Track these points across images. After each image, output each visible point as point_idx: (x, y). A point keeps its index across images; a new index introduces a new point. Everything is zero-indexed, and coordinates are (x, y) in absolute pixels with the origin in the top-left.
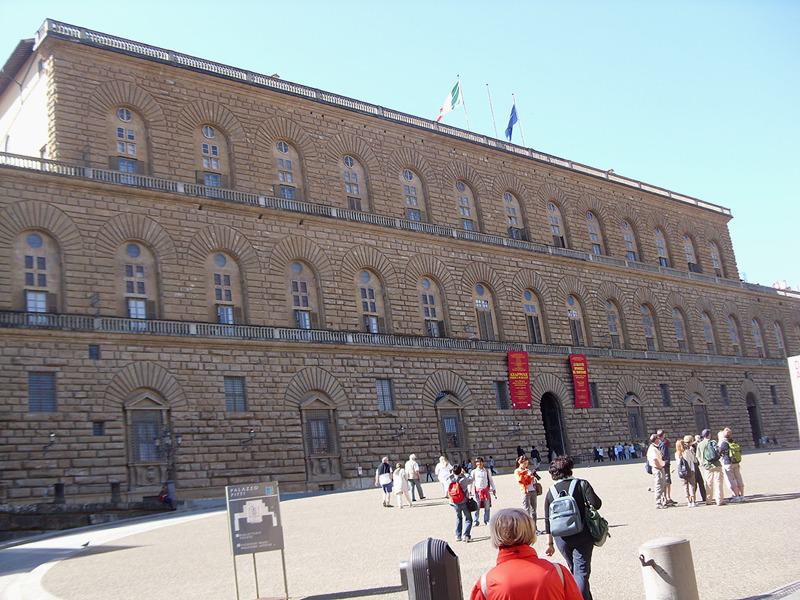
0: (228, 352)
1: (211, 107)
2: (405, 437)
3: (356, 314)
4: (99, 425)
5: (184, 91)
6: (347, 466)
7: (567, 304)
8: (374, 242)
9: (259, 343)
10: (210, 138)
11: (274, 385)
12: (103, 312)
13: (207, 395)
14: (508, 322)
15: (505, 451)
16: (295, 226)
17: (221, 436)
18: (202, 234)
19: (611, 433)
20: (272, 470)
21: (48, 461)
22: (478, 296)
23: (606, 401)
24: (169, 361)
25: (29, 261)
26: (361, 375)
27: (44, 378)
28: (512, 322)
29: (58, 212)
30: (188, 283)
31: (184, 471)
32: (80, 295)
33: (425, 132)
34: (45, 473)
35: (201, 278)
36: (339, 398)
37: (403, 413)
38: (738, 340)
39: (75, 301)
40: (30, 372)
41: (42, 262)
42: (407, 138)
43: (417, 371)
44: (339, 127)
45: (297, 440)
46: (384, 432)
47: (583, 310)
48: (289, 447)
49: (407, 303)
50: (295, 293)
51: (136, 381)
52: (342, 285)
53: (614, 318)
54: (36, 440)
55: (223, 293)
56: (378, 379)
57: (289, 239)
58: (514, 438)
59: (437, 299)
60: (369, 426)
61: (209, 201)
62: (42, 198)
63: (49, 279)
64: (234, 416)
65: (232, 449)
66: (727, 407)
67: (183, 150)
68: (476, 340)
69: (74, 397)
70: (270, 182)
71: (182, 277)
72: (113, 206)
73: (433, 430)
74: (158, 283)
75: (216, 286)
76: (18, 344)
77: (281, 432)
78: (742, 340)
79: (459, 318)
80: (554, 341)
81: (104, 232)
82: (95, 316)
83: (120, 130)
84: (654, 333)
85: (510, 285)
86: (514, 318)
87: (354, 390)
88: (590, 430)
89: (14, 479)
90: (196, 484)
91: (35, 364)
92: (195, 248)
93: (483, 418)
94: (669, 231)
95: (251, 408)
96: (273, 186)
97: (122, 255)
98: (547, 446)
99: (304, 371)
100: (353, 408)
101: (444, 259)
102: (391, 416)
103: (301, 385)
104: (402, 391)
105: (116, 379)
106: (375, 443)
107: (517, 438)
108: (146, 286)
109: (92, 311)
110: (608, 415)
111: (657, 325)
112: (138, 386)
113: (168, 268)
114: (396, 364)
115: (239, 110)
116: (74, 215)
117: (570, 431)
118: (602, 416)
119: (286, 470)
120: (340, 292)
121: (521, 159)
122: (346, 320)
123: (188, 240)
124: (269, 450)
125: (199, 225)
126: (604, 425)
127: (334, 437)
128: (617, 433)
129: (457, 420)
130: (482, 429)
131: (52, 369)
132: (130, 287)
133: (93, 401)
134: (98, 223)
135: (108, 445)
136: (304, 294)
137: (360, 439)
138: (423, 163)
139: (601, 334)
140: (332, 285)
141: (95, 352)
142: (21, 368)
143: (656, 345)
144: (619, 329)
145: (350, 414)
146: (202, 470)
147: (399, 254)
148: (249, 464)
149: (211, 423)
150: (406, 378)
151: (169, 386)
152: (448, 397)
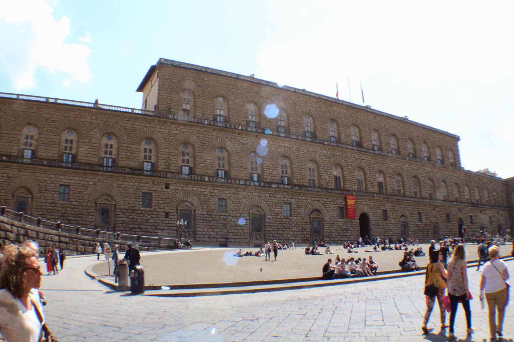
0: (221, 189)
3: (278, 175)
4: (167, 215)
5: (211, 83)
6: (268, 238)
8: (288, 146)
12: (171, 170)
15: (340, 237)
16: (254, 138)
17: (215, 222)
18: (214, 140)
19: (391, 232)
20: (235, 237)
24: (196, 191)
25: (146, 150)
29: (157, 132)
30: (206, 160)
31: (199, 234)
32: (163, 164)
34: (146, 230)
36: (267, 209)
37: (295, 218)
39: (161, 166)
40: (143, 193)
41: (150, 151)
42: (308, 101)
43: (303, 201)
47: (385, 178)
53: (400, 182)
54: (144, 218)
55: (221, 165)
56: (285, 203)
57: (251, 143)
58: (345, 232)
63: (153, 158)
64: (221, 214)
66: (448, 224)
68: (332, 189)
69: (158, 203)
70: (244, 119)
73: (308, 226)
74: (195, 160)
75: (218, 162)
80: (368, 191)
82: (168, 172)
83: (185, 99)
84: (418, 190)
87: (274, 207)
91: (145, 190)
92: (210, 147)
94: (430, 144)
96: (246, 121)
97: (181, 148)
99: (252, 198)
100: (273, 214)
102: (289, 219)
104: (295, 208)
105: (175, 197)
106: (281, 229)
107: (346, 231)
109: (167, 170)
111: (420, 186)
115: (234, 90)
117: (372, 230)
118: (388, 224)
122: (273, 178)
123: (208, 143)
124: (234, 229)
128: (394, 232)
129: (319, 223)
131: (151, 192)
132: (183, 161)
135: (170, 222)
140: (268, 163)
141: (167, 187)
142: (140, 191)
144: (401, 187)
145: (271, 217)
146: (206, 234)
149: (211, 216)
152: (316, 212)
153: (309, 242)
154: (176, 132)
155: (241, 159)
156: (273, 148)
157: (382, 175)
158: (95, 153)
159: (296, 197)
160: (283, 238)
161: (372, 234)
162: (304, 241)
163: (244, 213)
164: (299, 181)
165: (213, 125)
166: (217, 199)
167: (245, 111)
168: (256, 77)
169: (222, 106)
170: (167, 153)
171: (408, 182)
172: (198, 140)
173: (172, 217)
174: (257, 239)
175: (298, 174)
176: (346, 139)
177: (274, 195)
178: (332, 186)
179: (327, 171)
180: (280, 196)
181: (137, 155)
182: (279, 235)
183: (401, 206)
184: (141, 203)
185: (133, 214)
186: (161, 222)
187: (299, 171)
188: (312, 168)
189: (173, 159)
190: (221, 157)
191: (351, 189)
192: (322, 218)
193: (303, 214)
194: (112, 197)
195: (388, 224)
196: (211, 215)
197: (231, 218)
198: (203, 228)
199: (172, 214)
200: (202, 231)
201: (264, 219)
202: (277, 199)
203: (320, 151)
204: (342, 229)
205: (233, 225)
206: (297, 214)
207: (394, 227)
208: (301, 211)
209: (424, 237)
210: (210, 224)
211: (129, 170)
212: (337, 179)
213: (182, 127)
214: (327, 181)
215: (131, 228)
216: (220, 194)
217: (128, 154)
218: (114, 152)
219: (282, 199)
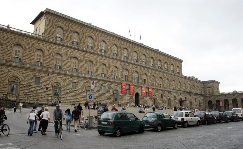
12: (50, 67)
13: (69, 85)
20: (79, 101)
25: (38, 55)
27: (38, 78)
32: (47, 63)
37: (107, 93)
39: (45, 64)
40: (35, 77)
54: (35, 90)
59: (117, 72)
78: (181, 87)
89: (30, 97)
94: (168, 63)
109: (48, 66)
113: (64, 60)
114: (106, 83)
119: (82, 101)
122: (98, 74)
125: (72, 52)
135: (49, 92)
141: (48, 75)
143: (162, 86)
145: (96, 92)
152: (116, 91)
154: (54, 48)
157: (146, 76)
164: (109, 76)
168: (92, 24)
177: (98, 82)
179: (122, 72)
194: (18, 78)
197: (78, 91)
213: (57, 46)
218: (21, 55)
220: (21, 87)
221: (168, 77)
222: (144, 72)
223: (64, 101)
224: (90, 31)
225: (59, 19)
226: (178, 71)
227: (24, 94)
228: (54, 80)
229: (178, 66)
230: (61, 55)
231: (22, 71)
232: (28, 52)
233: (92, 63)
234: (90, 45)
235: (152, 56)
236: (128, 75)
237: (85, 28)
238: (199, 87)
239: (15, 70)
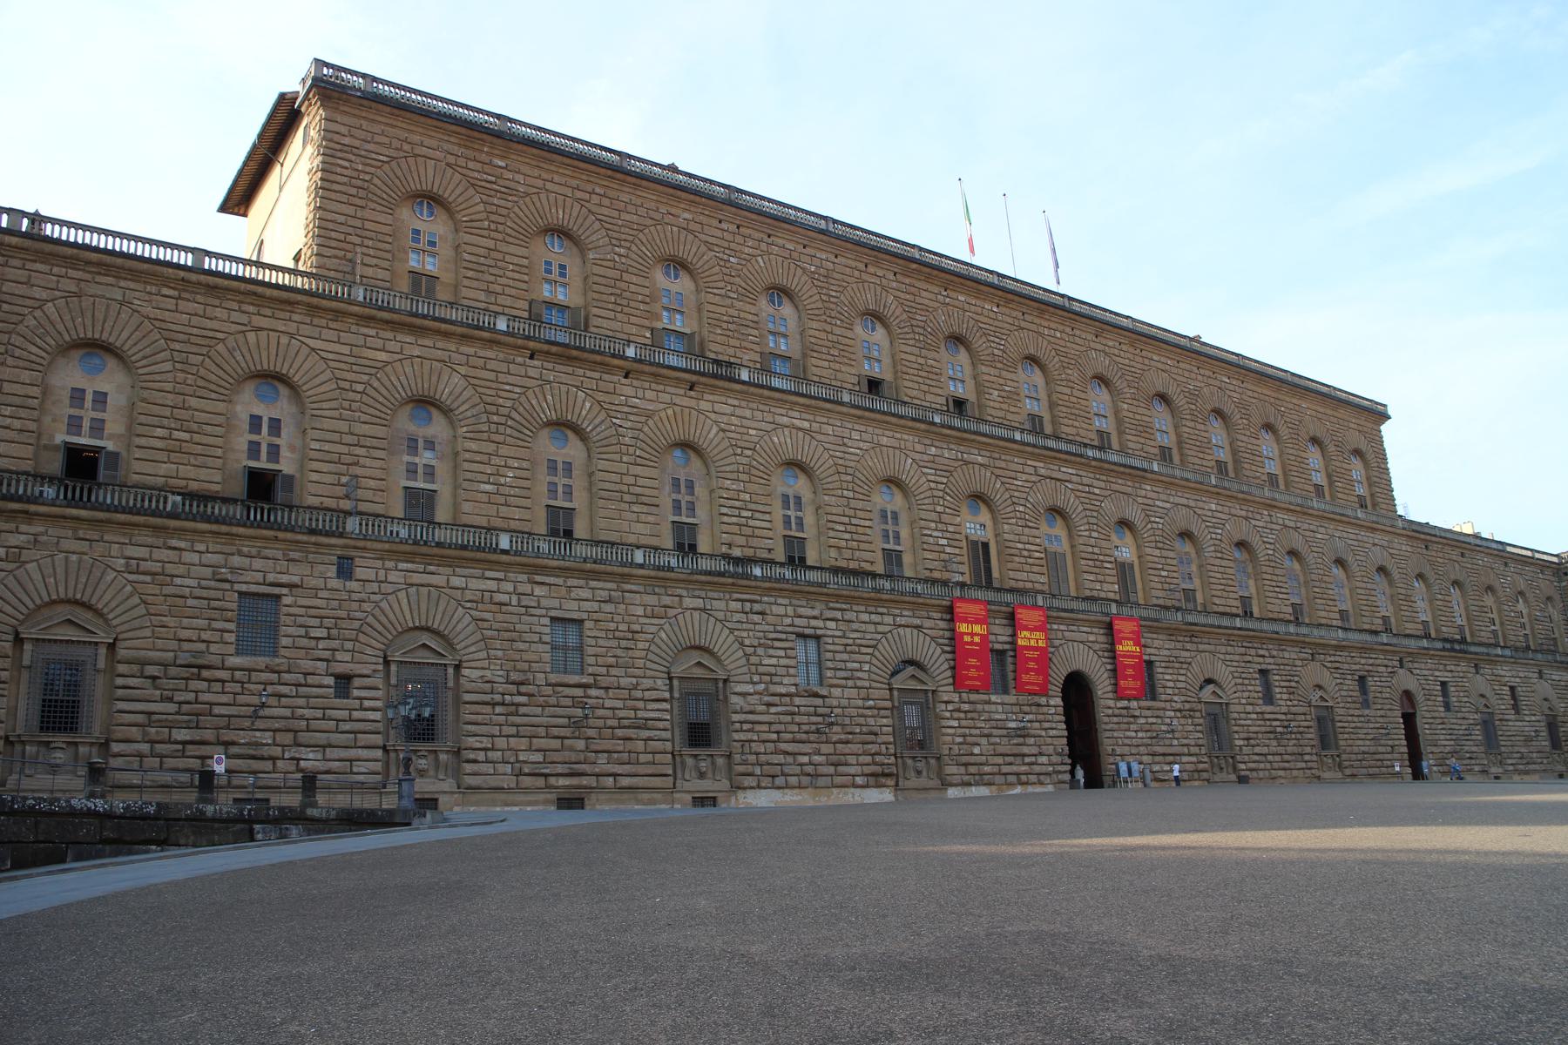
0: (560, 581)
1: (560, 203)
2: (835, 729)
6: (741, 769)
7: (1114, 537)
8: (806, 425)
9: (609, 568)
10: (554, 251)
11: (630, 636)
12: (363, 507)
13: (521, 646)
14: (1017, 559)
15: (1000, 760)
16: (682, 392)
21: (258, 734)
22: (969, 517)
23: (1169, 691)
26: (772, 628)
28: (1023, 560)
29: (305, 350)
30: (503, 471)
31: (475, 761)
33: (901, 262)
34: (251, 752)
35: (525, 464)
36: (733, 660)
37: (837, 692)
38: (1391, 608)
40: (241, 593)
41: (275, 426)
44: (763, 246)
45: (661, 725)
46: (805, 719)
48: (645, 734)
49: (854, 521)
50: (674, 496)
51: (408, 617)
52: (751, 487)
54: (241, 699)
55: (560, 489)
56: (800, 635)
57: (670, 412)
58: (1015, 741)
60: (779, 709)
61: (546, 347)
62: (283, 329)
63: (285, 452)
65: (555, 731)
66: (1367, 712)
67: (511, 267)
69: (307, 636)
70: (647, 323)
71: (495, 460)
72: (392, 346)
76: (227, 549)
77: (636, 709)
78: (1398, 609)
79: (937, 548)
80: (1088, 593)
81: (376, 384)
83: (417, 232)
84: (1253, 590)
85: (1022, 502)
86: (1026, 553)
87: (760, 651)
88: (1140, 735)
90: (494, 784)
92: (518, 417)
93: (966, 707)
94: (1284, 431)
95: (590, 670)
96: (652, 330)
98: (1069, 756)
99: (680, 617)
100: (756, 678)
101: (918, 456)
102: (816, 695)
103: (674, 639)
104: (838, 657)
105: (377, 612)
107: (1021, 740)
108: (438, 472)
109: (346, 505)
110: (1172, 714)
112: (411, 625)
113: (473, 446)
115: (605, 211)
116: (331, 356)
118: (1161, 713)
120: (747, 497)
121: (1052, 310)
122: (755, 542)
123: (509, 403)
126: (1164, 728)
127: (723, 723)
128: (1185, 741)
130: (964, 723)
131: (276, 590)
133: (335, 644)
134: (367, 370)
135: (356, 714)
136: (689, 498)
137: (765, 728)
138: (893, 307)
139: (1166, 587)
140: (734, 487)
141: (345, 569)
142: (227, 586)
145: (750, 688)
147: (844, 445)
148: (582, 757)
149: (523, 689)
150: (843, 637)
151: (460, 626)
152: (910, 670)
153: (891, 782)
154: (383, 356)
155: (638, 470)
156: (752, 432)
157: (1128, 538)
158: (17, 424)
159: (838, 615)
160: (797, 770)
161: (1110, 749)
162: (872, 779)
163: (649, 673)
164: (847, 554)
165: (528, 338)
166: (546, 621)
167: (646, 292)
169: (562, 267)
170: (348, 439)
171: (1217, 562)
172: (469, 392)
173: (364, 693)
174: (702, 775)
175: (842, 528)
176: (1005, 406)
177: (757, 607)
178: (962, 574)
179: (945, 518)
180: (781, 608)
181: (219, 441)
182: (780, 758)
183: (1201, 647)
184: (231, 638)
185: (194, 685)
186: (319, 713)
187: (846, 520)
188: (889, 508)
189: (368, 462)
190: (559, 460)
191: (1029, 585)
192: (934, 691)
193: (865, 676)
195: (1161, 713)
196: (522, 683)
197: (601, 693)
198: (493, 736)
199: (367, 681)
200: (485, 749)
201: (726, 698)
202: (770, 619)
203: (919, 447)
204: (1004, 732)
205: (610, 723)
206: (846, 679)
207: (1183, 721)
208: (856, 665)
209: (1286, 757)
210: (517, 720)
211: (179, 498)
212: (980, 551)
214: (946, 557)
215: (184, 743)
216: (556, 603)
217: (176, 434)
219: (788, 621)
220: (120, 681)
221: (1297, 542)
222: (1112, 509)
223: (493, 781)
224: (668, 219)
225: (416, 138)
226: (1361, 490)
227: (152, 742)
228: (402, 610)
229: (1357, 452)
230: (446, 412)
231: (132, 551)
232: (170, 399)
233: (696, 463)
234: (678, 324)
235: (1160, 382)
236: (988, 535)
237: (625, 198)
238: (1530, 595)
239: (68, 544)
